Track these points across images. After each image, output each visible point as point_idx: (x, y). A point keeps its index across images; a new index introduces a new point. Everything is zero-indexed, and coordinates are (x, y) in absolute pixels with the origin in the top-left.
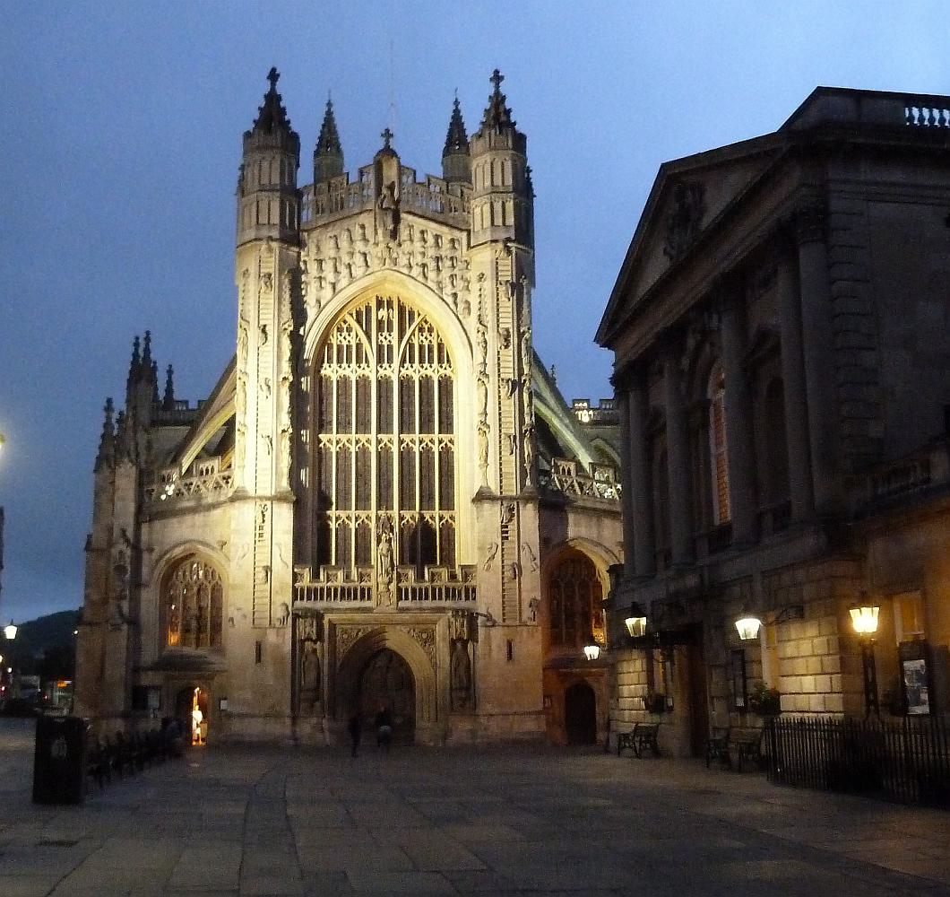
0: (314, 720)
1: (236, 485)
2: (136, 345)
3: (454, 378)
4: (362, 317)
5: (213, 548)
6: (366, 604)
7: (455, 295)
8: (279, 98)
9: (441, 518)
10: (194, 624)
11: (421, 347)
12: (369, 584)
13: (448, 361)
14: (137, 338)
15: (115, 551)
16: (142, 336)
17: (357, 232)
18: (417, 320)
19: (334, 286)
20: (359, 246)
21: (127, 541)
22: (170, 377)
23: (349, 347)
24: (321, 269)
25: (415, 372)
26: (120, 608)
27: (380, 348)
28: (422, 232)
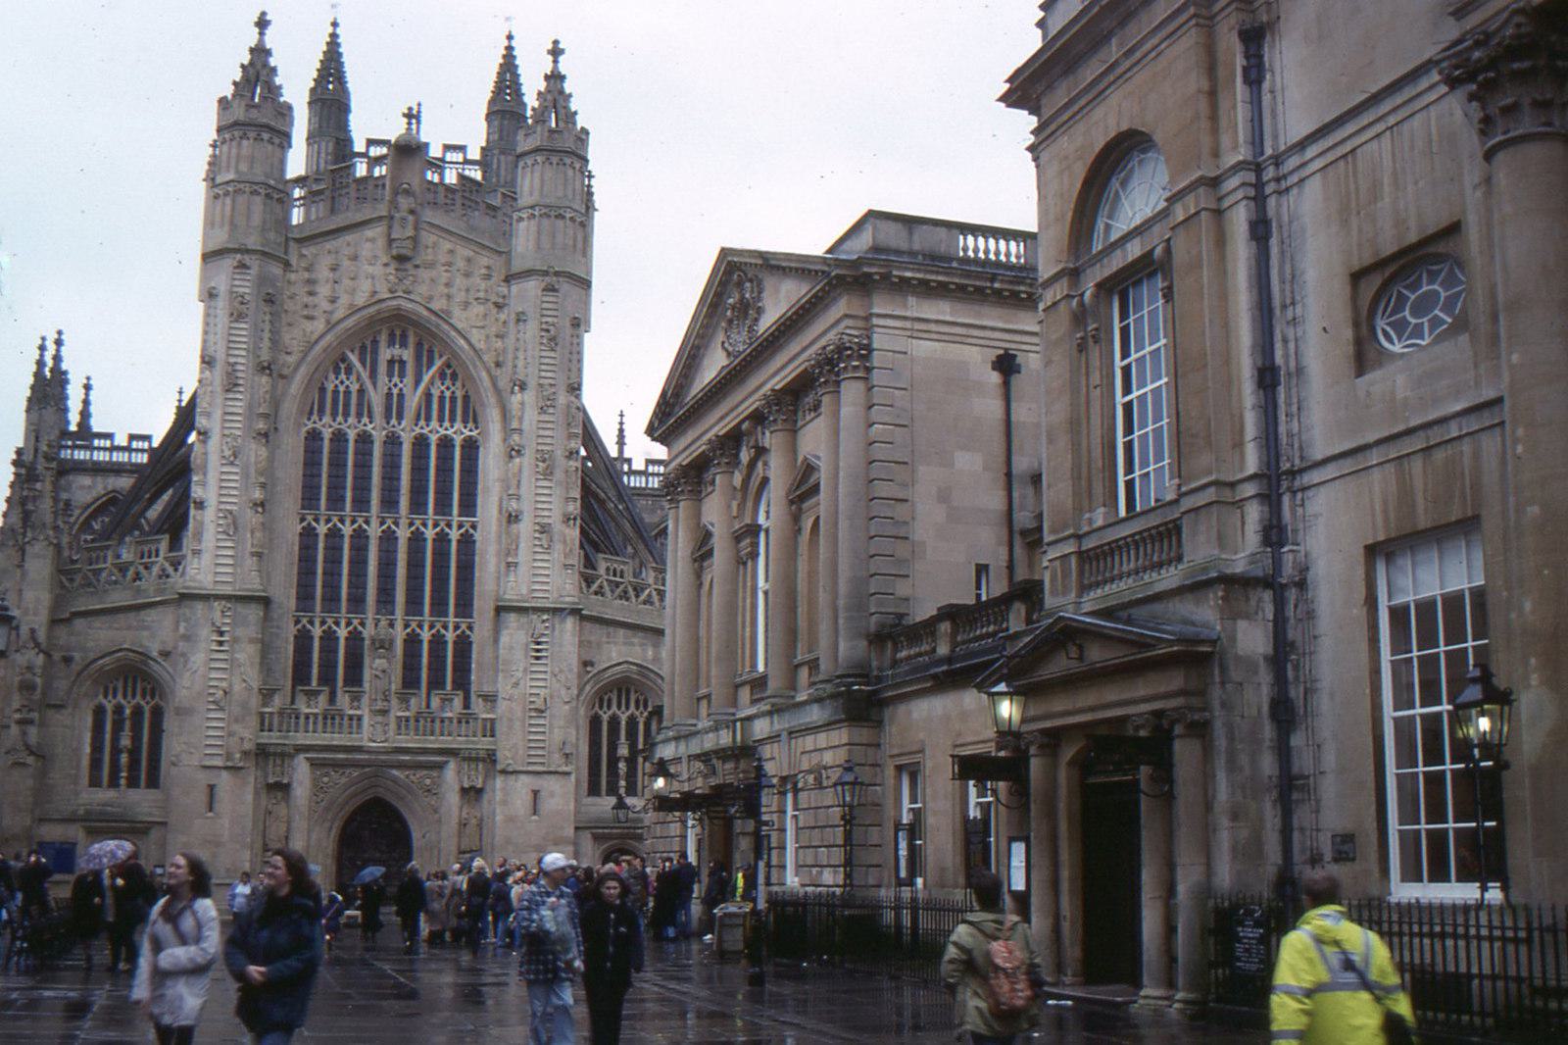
2: (42, 348)
4: (368, 353)
9: (457, 627)
10: (124, 758)
11: (442, 398)
12: (358, 712)
13: (475, 421)
14: (43, 339)
16: (52, 337)
18: (438, 363)
21: (37, 645)
22: (87, 395)
23: (347, 393)
25: (435, 431)
27: (389, 395)
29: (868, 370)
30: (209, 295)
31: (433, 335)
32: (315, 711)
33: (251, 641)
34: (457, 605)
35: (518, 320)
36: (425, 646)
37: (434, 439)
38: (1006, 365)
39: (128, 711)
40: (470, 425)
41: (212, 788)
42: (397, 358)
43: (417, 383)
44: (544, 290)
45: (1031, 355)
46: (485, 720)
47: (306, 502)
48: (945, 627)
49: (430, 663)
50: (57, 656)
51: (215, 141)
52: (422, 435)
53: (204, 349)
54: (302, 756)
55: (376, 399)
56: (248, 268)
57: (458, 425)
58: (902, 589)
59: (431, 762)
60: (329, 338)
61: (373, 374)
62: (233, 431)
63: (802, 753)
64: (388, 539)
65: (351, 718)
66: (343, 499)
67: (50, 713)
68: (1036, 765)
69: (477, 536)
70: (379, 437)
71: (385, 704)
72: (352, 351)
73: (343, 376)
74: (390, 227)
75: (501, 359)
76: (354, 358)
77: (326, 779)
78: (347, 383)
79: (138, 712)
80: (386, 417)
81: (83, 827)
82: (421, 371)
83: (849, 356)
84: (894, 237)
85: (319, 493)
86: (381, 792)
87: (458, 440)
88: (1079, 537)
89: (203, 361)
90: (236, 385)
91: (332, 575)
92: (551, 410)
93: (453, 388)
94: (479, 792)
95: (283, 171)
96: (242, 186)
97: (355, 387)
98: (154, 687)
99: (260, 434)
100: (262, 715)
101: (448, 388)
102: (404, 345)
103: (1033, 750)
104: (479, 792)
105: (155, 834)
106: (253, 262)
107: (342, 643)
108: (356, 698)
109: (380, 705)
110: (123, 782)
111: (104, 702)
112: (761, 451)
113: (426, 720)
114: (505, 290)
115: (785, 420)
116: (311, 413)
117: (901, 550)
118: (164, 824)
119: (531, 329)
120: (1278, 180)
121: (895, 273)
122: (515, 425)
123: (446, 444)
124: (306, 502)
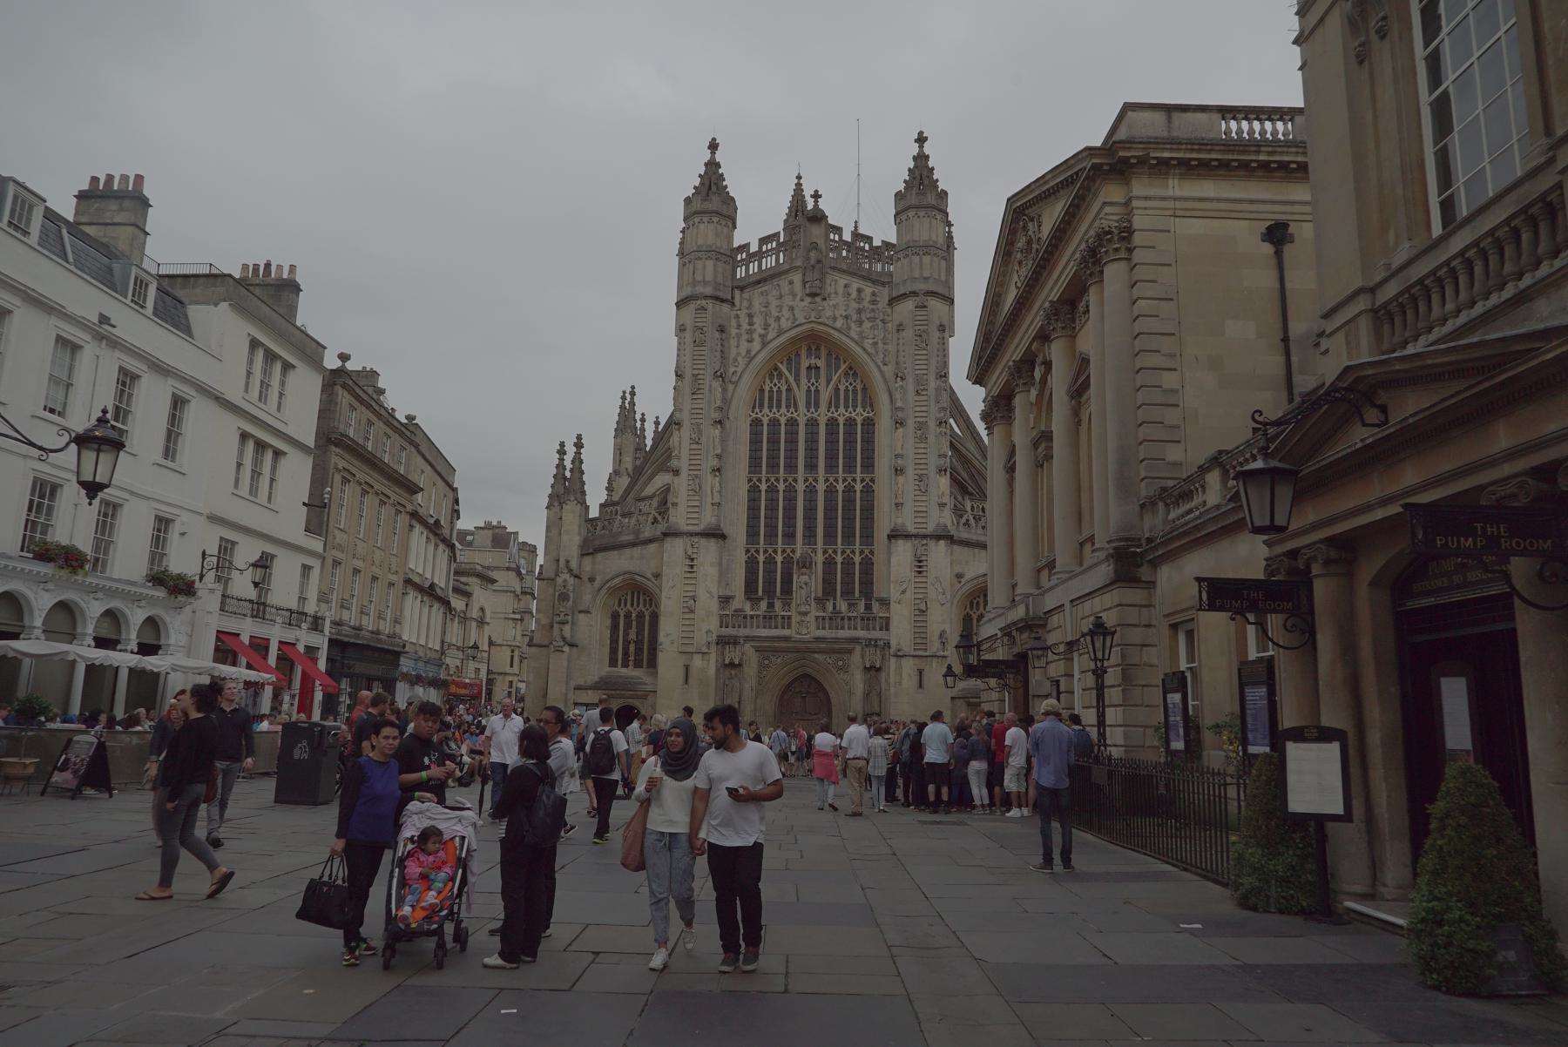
1: (671, 519)
2: (624, 398)
5: (648, 579)
6: (786, 632)
7: (875, 344)
8: (718, 165)
10: (632, 648)
11: (847, 391)
13: (871, 405)
14: (624, 392)
15: (559, 581)
16: (629, 390)
17: (785, 288)
18: (843, 367)
19: (761, 336)
20: (787, 301)
21: (570, 570)
23: (779, 391)
24: (751, 324)
25: (842, 415)
27: (809, 391)
28: (846, 286)
29: (1130, 250)
30: (681, 329)
32: (758, 613)
34: (861, 537)
36: (839, 566)
37: (841, 420)
38: (1277, 234)
40: (869, 409)
41: (687, 668)
42: (813, 365)
43: (828, 382)
45: (1304, 224)
48: (1214, 478)
50: (585, 577)
53: (677, 367)
54: (748, 647)
57: (859, 409)
58: (1174, 454)
59: (842, 650)
60: (763, 354)
61: (797, 379)
63: (1082, 619)
64: (811, 491)
65: (783, 617)
67: (581, 616)
68: (1322, 590)
69: (875, 487)
70: (802, 421)
73: (776, 381)
74: (804, 275)
75: (887, 359)
77: (767, 662)
79: (641, 616)
84: (1152, 126)
85: (761, 462)
86: (809, 671)
87: (859, 420)
88: (1372, 290)
89: (677, 375)
91: (772, 518)
94: (879, 669)
95: (730, 239)
96: (700, 254)
97: (784, 388)
100: (721, 616)
101: (851, 384)
103: (1316, 569)
104: (879, 669)
105: (650, 699)
106: (709, 304)
107: (779, 564)
108: (787, 604)
109: (803, 609)
110: (631, 663)
112: (1048, 365)
113: (836, 619)
114: (889, 310)
115: (1063, 328)
116: (754, 407)
117: (1172, 416)
119: (908, 334)
121: (1152, 155)
122: (899, 404)
123: (850, 423)
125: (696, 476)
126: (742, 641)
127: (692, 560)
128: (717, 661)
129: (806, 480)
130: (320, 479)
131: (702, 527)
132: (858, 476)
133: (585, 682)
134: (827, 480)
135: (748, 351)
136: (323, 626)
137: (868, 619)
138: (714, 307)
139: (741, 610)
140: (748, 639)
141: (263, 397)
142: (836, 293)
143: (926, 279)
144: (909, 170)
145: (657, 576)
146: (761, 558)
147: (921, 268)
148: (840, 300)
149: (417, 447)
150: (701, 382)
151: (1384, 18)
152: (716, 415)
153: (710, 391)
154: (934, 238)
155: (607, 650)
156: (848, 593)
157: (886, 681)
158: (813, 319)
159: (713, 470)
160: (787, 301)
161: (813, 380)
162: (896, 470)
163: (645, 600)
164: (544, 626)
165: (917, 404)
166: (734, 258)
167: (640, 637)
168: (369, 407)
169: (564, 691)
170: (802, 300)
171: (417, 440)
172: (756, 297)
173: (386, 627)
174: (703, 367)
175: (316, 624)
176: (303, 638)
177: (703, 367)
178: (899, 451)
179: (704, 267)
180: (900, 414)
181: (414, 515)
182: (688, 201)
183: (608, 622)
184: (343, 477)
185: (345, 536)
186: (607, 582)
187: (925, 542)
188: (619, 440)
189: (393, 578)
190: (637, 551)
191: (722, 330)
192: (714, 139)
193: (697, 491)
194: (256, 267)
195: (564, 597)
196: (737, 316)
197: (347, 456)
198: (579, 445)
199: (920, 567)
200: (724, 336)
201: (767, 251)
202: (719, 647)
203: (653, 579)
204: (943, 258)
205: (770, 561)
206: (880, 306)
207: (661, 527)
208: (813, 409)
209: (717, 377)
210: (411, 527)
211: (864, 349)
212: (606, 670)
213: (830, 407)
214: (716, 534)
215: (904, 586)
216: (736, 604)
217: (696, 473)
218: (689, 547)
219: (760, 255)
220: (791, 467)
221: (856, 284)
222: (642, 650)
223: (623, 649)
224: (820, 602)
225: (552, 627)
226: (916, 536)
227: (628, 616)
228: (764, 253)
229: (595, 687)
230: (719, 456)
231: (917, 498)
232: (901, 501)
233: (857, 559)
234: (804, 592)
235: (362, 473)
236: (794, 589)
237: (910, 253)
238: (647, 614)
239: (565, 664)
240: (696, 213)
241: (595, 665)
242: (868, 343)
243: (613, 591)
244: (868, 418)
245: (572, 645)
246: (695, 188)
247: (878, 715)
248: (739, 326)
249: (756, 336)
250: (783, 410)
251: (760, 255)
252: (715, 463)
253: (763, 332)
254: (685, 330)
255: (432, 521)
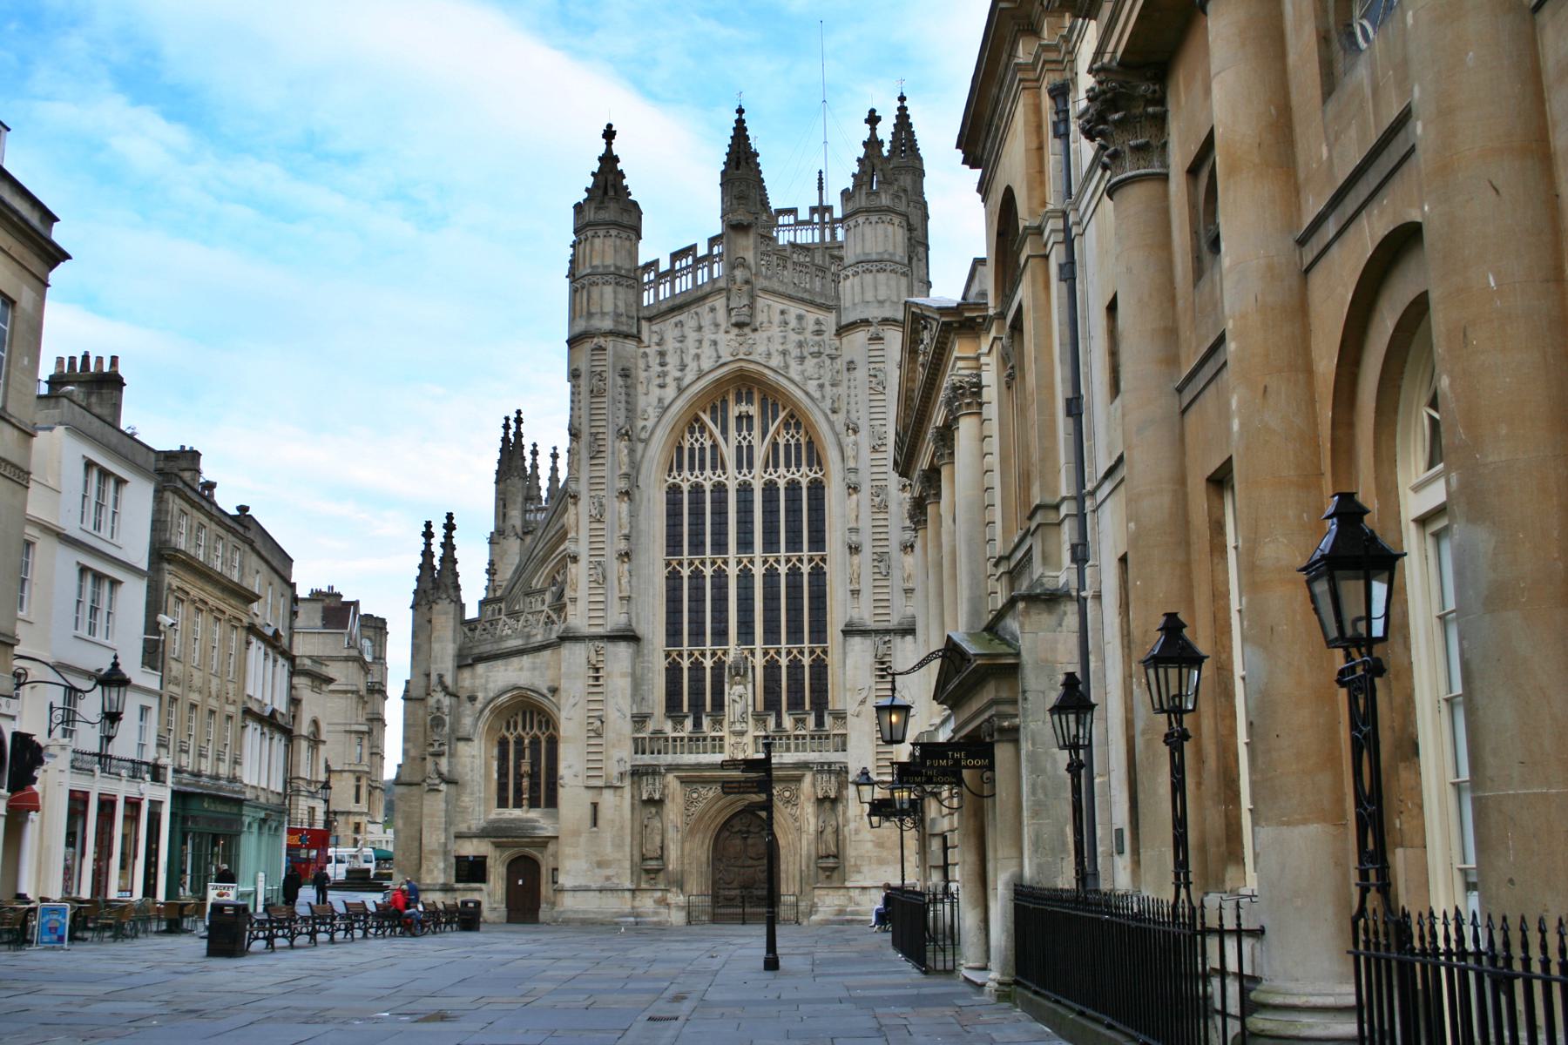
0: (659, 894)
2: (506, 427)
3: (825, 480)
5: (543, 696)
7: (821, 386)
8: (616, 159)
10: (526, 782)
11: (788, 446)
13: (819, 464)
14: (507, 419)
15: (431, 701)
16: (513, 416)
18: (782, 415)
19: (678, 379)
21: (445, 689)
22: (555, 463)
23: (702, 449)
24: (663, 364)
25: (782, 476)
26: (437, 764)
27: (739, 448)
28: (783, 312)
29: (981, 405)
30: (574, 375)
31: (776, 391)
32: (681, 734)
33: (623, 675)
35: (848, 369)
37: (782, 484)
39: (526, 741)
41: (595, 806)
44: (870, 339)
46: (835, 735)
47: (671, 549)
49: (789, 686)
50: (463, 696)
51: (574, 242)
52: (771, 481)
54: (670, 777)
55: (729, 454)
56: (605, 350)
57: (804, 469)
61: (724, 431)
62: (598, 492)
64: (746, 576)
65: (714, 739)
66: (703, 543)
67: (461, 746)
69: (827, 568)
71: (744, 725)
72: (704, 412)
73: (697, 435)
74: (728, 299)
75: (836, 405)
76: (706, 418)
77: (695, 795)
78: (701, 440)
79: (535, 742)
80: (737, 468)
81: (493, 843)
82: (768, 424)
83: (962, 395)
85: (681, 541)
87: (804, 483)
89: (571, 434)
90: (599, 452)
92: (883, 449)
93: (797, 436)
95: (634, 255)
96: (595, 279)
97: (708, 444)
98: (548, 721)
99: (621, 493)
100: (635, 740)
101: (793, 437)
102: (750, 401)
104: (834, 801)
105: (551, 847)
106: (609, 344)
108: (717, 722)
109: (738, 727)
111: (507, 734)
116: (671, 470)
118: (557, 838)
119: (861, 374)
120: (1079, 224)
122: (852, 464)
123: (793, 487)
124: (671, 549)
125: (599, 563)
126: (663, 771)
127: (597, 670)
128: (633, 797)
129: (739, 562)
130: (154, 606)
131: (608, 629)
132: (805, 553)
133: (469, 828)
134: (765, 562)
135: (660, 400)
136: (165, 775)
137: (820, 738)
138: (614, 347)
139: (660, 732)
140: (671, 768)
141: (98, 526)
142: (770, 322)
143: (881, 303)
144: (859, 160)
145: (554, 691)
146: (686, 664)
147: (876, 288)
148: (775, 331)
149: (251, 544)
150: (601, 443)
151: (1012, 368)
152: (623, 485)
153: (613, 453)
154: (891, 250)
155: (494, 786)
156: (796, 704)
157: (844, 813)
158: (741, 356)
159: (620, 555)
160: (708, 335)
161: (745, 433)
162: (850, 547)
163: (540, 722)
164: (414, 759)
165: (874, 463)
166: (638, 280)
167: (536, 769)
168: (200, 508)
169: (443, 840)
170: (727, 332)
171: (250, 535)
172: (668, 328)
173: (224, 769)
174: (603, 423)
175: (156, 773)
176: (149, 791)
177: (603, 423)
178: (853, 525)
179: (602, 295)
180: (852, 477)
181: (252, 629)
182: (578, 208)
183: (495, 752)
184: (177, 597)
185: (180, 666)
186: (492, 700)
187: (887, 638)
188: (502, 486)
189: (231, 709)
190: (526, 660)
191: (626, 374)
192: (610, 126)
193: (601, 580)
194: (72, 360)
195: (438, 722)
196: (645, 355)
197: (181, 573)
198: (450, 527)
199: (882, 670)
200: (629, 381)
201: (682, 269)
202: (636, 778)
203: (549, 696)
204: (904, 274)
205: (697, 667)
206: (826, 337)
207: (557, 630)
208: (745, 470)
209: (623, 435)
210: (248, 643)
211: (807, 393)
212: (496, 813)
213: (767, 466)
214: (629, 636)
215: (864, 694)
216: (651, 726)
217: (598, 559)
218: (593, 654)
219: (671, 274)
220: (720, 546)
221: (794, 310)
222: (538, 784)
223: (515, 784)
224: (760, 719)
225: (424, 759)
226: (877, 632)
227: (519, 741)
228: (678, 271)
229: (483, 834)
230: (627, 537)
231: (877, 583)
232: (857, 587)
233: (806, 661)
234: (736, 705)
235: (196, 590)
236: (726, 703)
237: (860, 270)
238: (543, 739)
239: (443, 805)
240: (589, 225)
241: (480, 807)
242: (812, 386)
243: (499, 712)
244: (816, 479)
245: (451, 782)
246: (587, 190)
247: (835, 857)
248: (648, 367)
249: (669, 380)
250: (708, 472)
251: (671, 274)
252: (623, 546)
253: (678, 374)
254: (579, 376)
255: (269, 632)
